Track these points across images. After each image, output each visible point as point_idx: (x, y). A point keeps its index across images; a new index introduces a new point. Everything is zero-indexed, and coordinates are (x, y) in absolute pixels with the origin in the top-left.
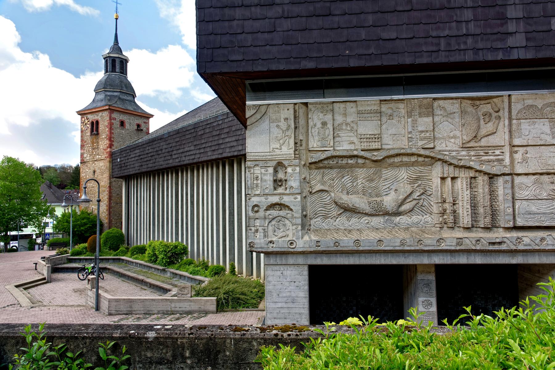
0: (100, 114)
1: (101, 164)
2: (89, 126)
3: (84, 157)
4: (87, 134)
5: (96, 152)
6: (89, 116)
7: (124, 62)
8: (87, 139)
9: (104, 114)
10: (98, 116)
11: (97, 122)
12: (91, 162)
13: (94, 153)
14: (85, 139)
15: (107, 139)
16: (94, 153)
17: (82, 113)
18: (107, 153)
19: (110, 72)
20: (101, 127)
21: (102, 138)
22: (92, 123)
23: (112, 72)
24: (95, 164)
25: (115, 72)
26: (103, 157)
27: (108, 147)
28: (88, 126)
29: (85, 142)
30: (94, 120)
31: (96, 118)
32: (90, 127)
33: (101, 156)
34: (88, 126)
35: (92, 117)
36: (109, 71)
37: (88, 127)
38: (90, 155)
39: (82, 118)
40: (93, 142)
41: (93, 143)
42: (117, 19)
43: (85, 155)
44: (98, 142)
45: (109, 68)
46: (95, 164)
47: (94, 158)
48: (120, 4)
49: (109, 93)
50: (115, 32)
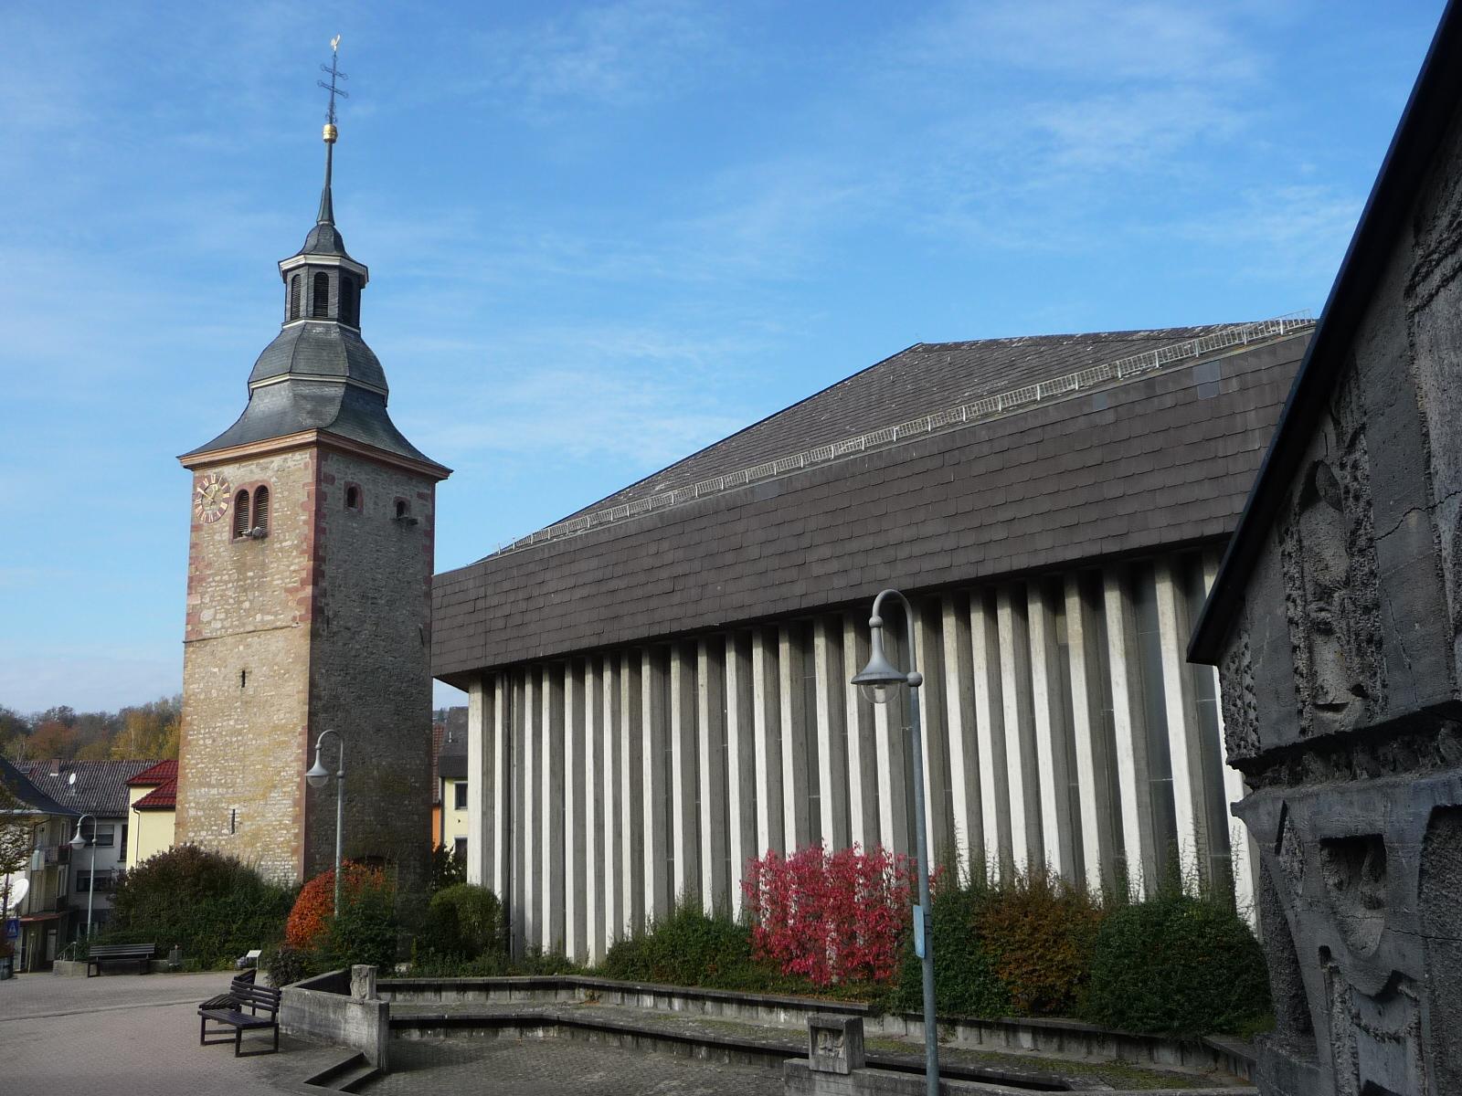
0: (277, 461)
1: (277, 643)
2: (229, 508)
3: (200, 622)
4: (217, 537)
5: (251, 602)
6: (229, 471)
7: (353, 282)
8: (218, 555)
9: (290, 463)
10: (265, 469)
11: (262, 492)
12: (230, 640)
13: (247, 605)
14: (209, 553)
15: (303, 552)
16: (247, 605)
17: (198, 464)
18: (300, 602)
19: (307, 317)
20: (278, 508)
21: (281, 550)
22: (242, 496)
23: (315, 316)
24: (248, 646)
25: (325, 316)
26: (283, 619)
27: (303, 583)
28: (224, 506)
29: (209, 565)
30: (251, 484)
31: (256, 477)
32: (231, 511)
33: (276, 614)
34: (224, 506)
35: (240, 476)
36: (302, 313)
37: (223, 512)
38: (227, 612)
39: (197, 481)
40: (244, 564)
41: (241, 567)
42: (332, 141)
43: (206, 615)
44: (263, 566)
45: (303, 302)
46: (248, 646)
47: (244, 625)
48: (341, 93)
49: (306, 390)
50: (324, 185)
